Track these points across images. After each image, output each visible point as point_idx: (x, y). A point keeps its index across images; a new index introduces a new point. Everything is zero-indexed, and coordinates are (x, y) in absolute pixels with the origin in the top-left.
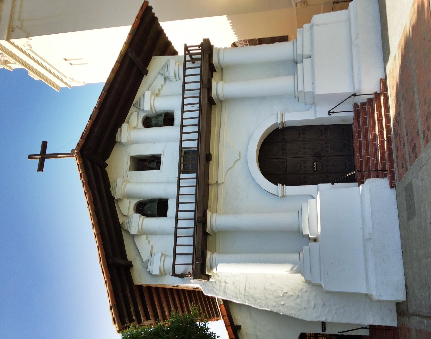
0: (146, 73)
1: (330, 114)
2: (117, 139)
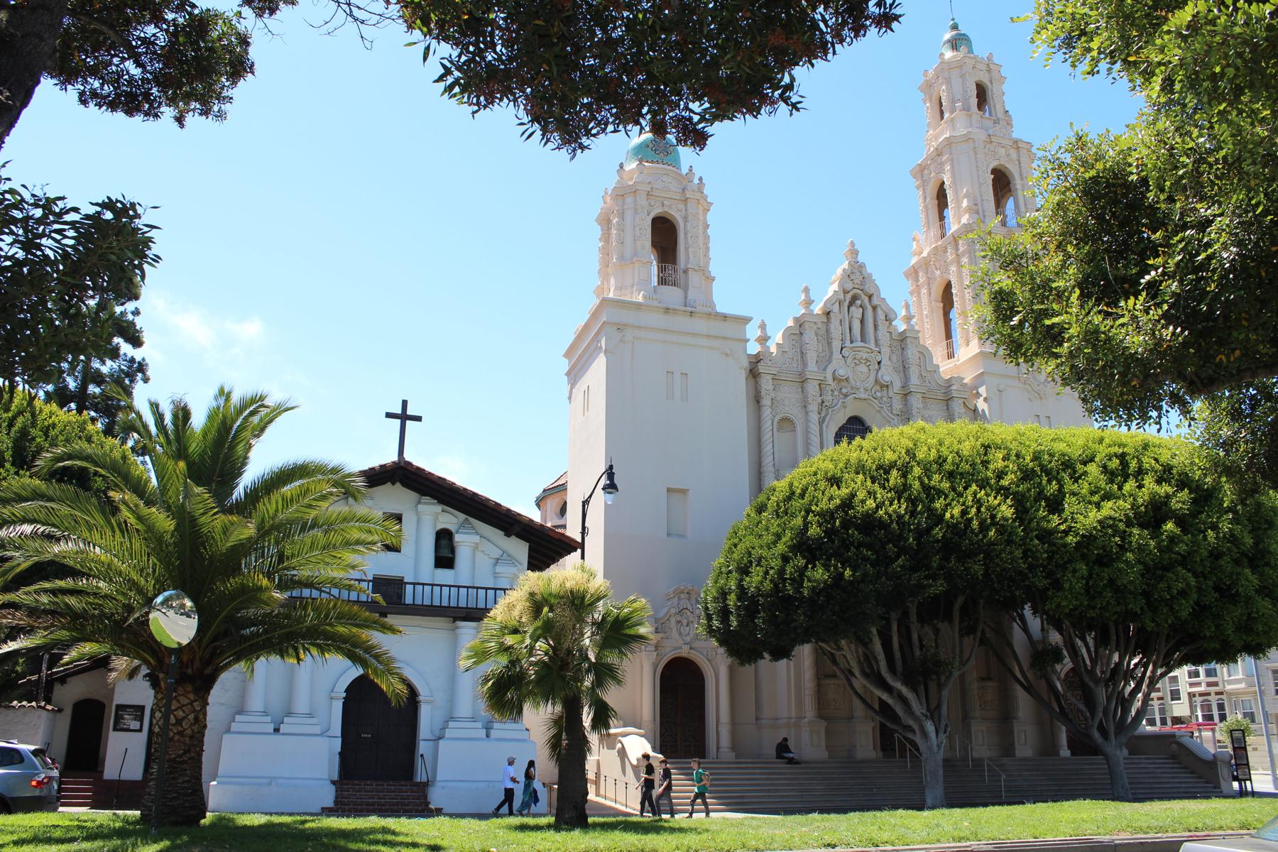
0: (508, 534)
1: (422, 756)
2: (426, 499)
